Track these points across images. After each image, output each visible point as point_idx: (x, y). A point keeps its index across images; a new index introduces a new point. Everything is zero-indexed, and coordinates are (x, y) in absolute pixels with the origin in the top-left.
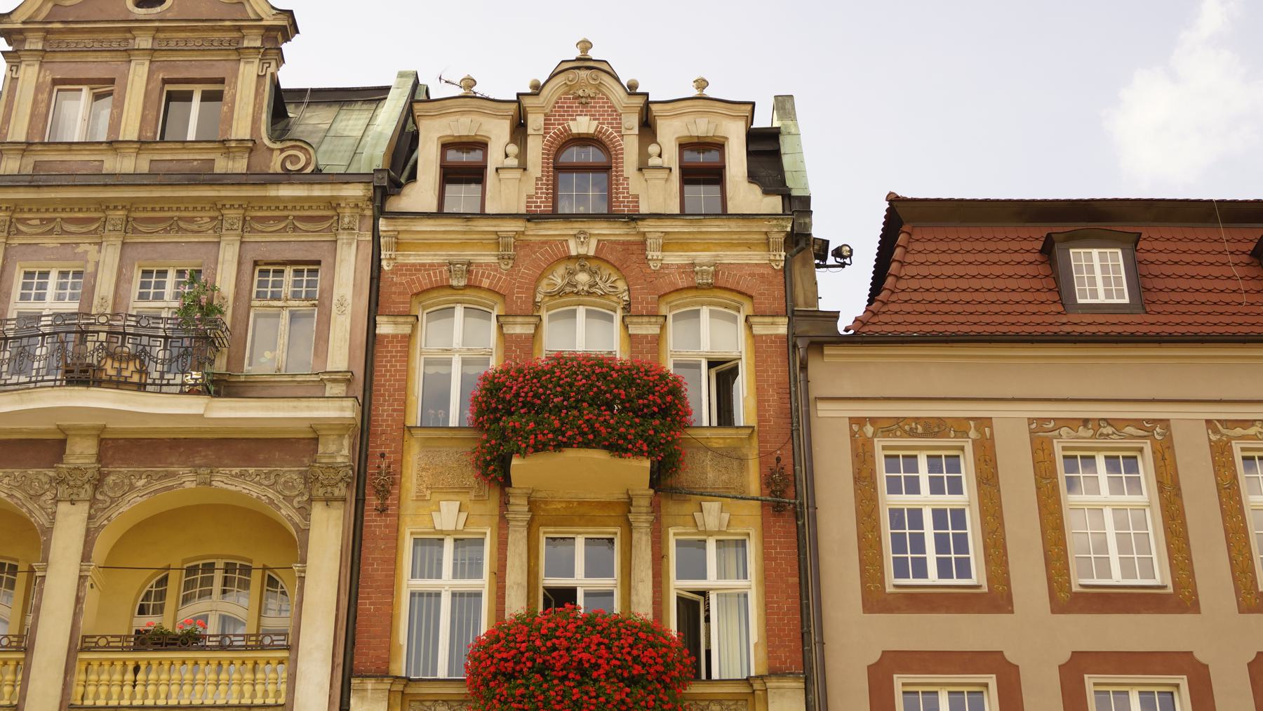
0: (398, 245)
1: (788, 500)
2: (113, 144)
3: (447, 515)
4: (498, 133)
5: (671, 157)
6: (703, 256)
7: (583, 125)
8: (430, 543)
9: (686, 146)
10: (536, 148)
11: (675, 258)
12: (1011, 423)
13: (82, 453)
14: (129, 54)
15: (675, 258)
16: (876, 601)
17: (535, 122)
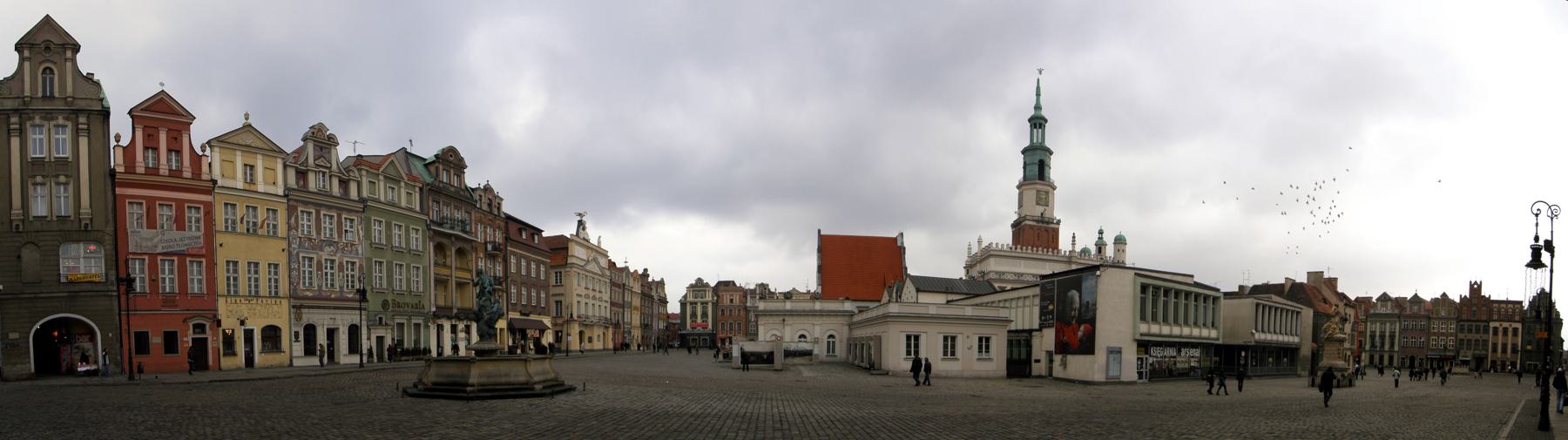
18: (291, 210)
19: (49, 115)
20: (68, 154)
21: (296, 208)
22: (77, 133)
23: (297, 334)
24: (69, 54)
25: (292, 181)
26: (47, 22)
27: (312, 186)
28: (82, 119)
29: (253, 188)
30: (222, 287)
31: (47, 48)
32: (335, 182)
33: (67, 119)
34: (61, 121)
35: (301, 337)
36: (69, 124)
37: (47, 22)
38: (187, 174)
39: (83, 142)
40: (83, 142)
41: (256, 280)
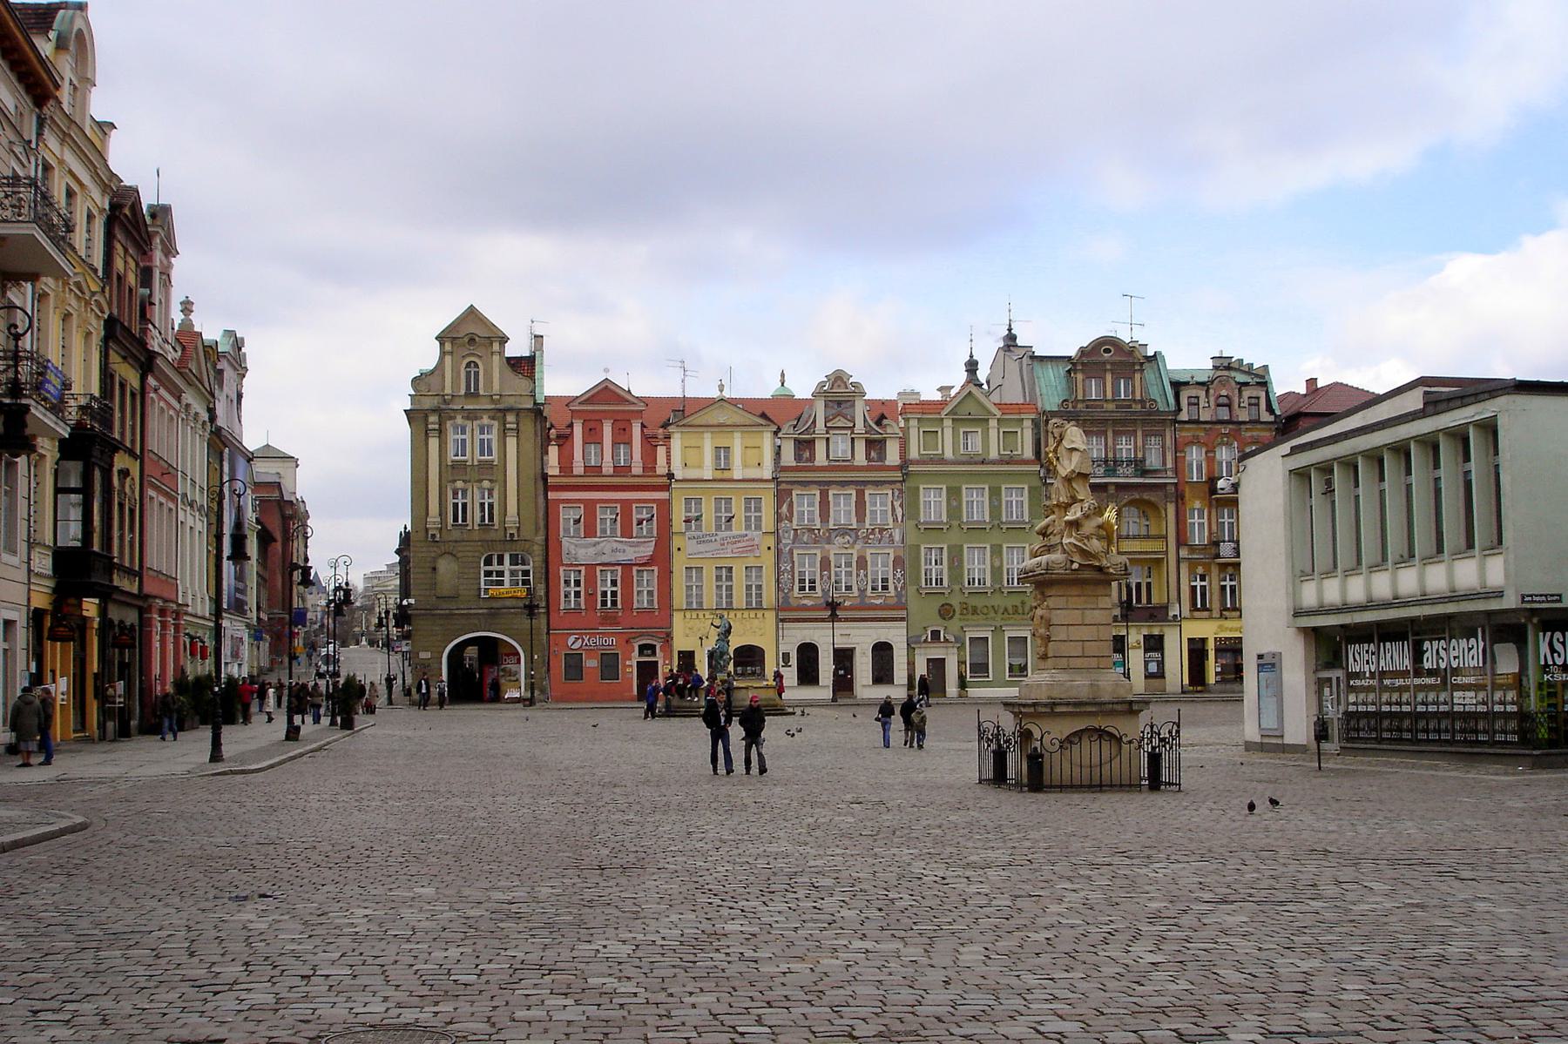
0: (1181, 430)
3: (1197, 504)
4: (1202, 394)
7: (1224, 392)
10: (1212, 399)
13: (1112, 490)
18: (782, 496)
19: (472, 415)
20: (495, 456)
22: (504, 432)
23: (786, 657)
24: (496, 347)
25: (788, 458)
26: (472, 312)
27: (820, 458)
28: (511, 418)
29: (726, 475)
30: (679, 598)
31: (472, 341)
32: (860, 447)
33: (493, 418)
34: (486, 420)
35: (794, 661)
36: (496, 423)
37: (472, 312)
38: (637, 469)
39: (511, 443)
40: (511, 443)
41: (729, 588)
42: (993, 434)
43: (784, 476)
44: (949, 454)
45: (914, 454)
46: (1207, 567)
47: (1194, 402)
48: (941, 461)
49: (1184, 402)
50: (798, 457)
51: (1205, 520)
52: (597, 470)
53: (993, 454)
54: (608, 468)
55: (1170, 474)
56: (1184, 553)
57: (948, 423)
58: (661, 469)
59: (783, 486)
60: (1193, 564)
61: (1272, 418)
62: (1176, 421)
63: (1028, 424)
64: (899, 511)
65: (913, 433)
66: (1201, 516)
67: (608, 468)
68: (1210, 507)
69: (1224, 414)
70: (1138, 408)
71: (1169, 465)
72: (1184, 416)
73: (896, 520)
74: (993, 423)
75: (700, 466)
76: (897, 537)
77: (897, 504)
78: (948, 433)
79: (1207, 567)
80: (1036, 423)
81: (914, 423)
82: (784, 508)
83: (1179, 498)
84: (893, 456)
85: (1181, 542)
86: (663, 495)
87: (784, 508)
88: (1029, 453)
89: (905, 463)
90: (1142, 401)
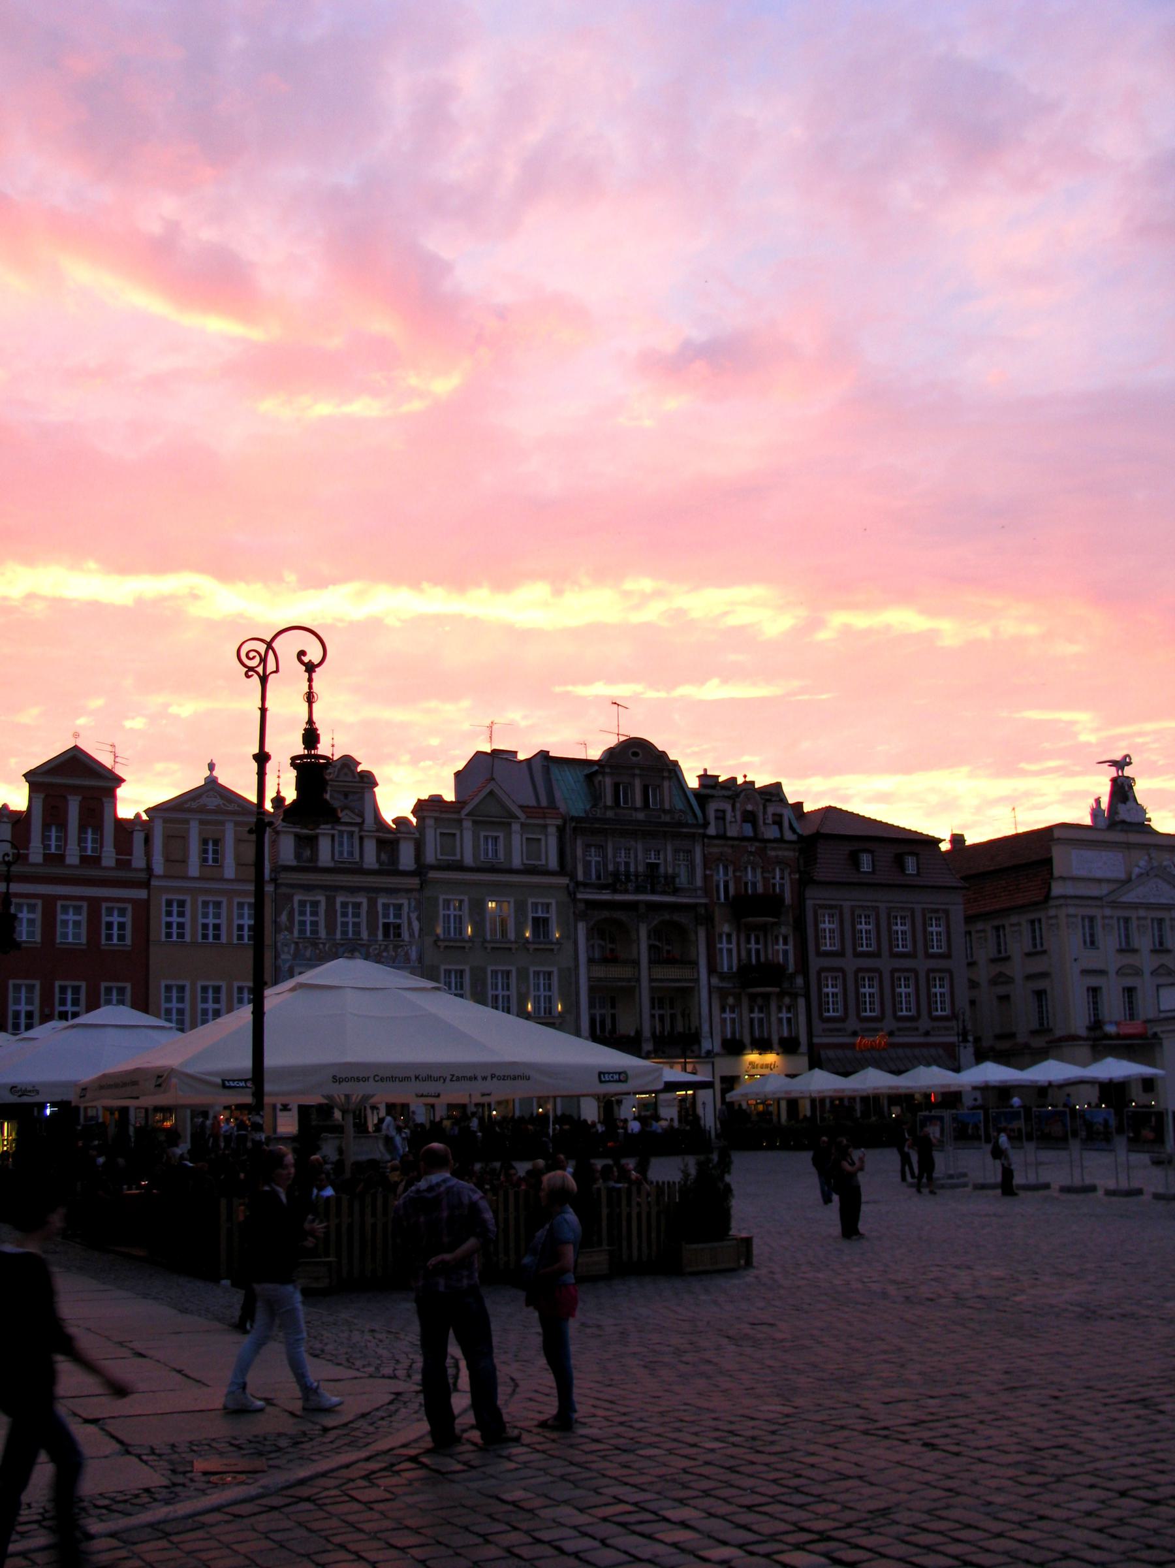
1: (799, 926)
2: (636, 809)
3: (726, 928)
4: (728, 808)
5: (770, 821)
6: (780, 853)
7: (749, 807)
8: (720, 936)
9: (774, 815)
10: (738, 814)
11: (773, 853)
12: (847, 905)
14: (634, 775)
15: (773, 853)
16: (819, 954)
17: (738, 805)
21: (290, 898)
27: (325, 856)
32: (370, 847)
38: (109, 857)
42: (516, 840)
43: (284, 877)
44: (468, 860)
45: (430, 857)
46: (738, 998)
47: (721, 816)
48: (460, 867)
49: (712, 815)
50: (298, 856)
51: (733, 946)
52: (60, 859)
53: (517, 862)
54: (73, 858)
55: (699, 892)
56: (715, 981)
57: (467, 824)
58: (138, 861)
59: (283, 890)
60: (723, 994)
61: (793, 837)
62: (705, 836)
63: (552, 830)
64: (416, 925)
65: (430, 835)
66: (729, 942)
67: (73, 858)
68: (739, 931)
69: (748, 830)
70: (666, 818)
71: (699, 882)
72: (712, 831)
73: (412, 935)
74: (516, 827)
75: (184, 861)
76: (414, 955)
77: (414, 916)
78: (468, 836)
79: (738, 998)
80: (561, 830)
81: (430, 822)
82: (284, 918)
83: (708, 921)
84: (406, 858)
85: (712, 970)
86: (142, 894)
87: (284, 918)
88: (553, 863)
89: (421, 870)
90: (669, 812)
